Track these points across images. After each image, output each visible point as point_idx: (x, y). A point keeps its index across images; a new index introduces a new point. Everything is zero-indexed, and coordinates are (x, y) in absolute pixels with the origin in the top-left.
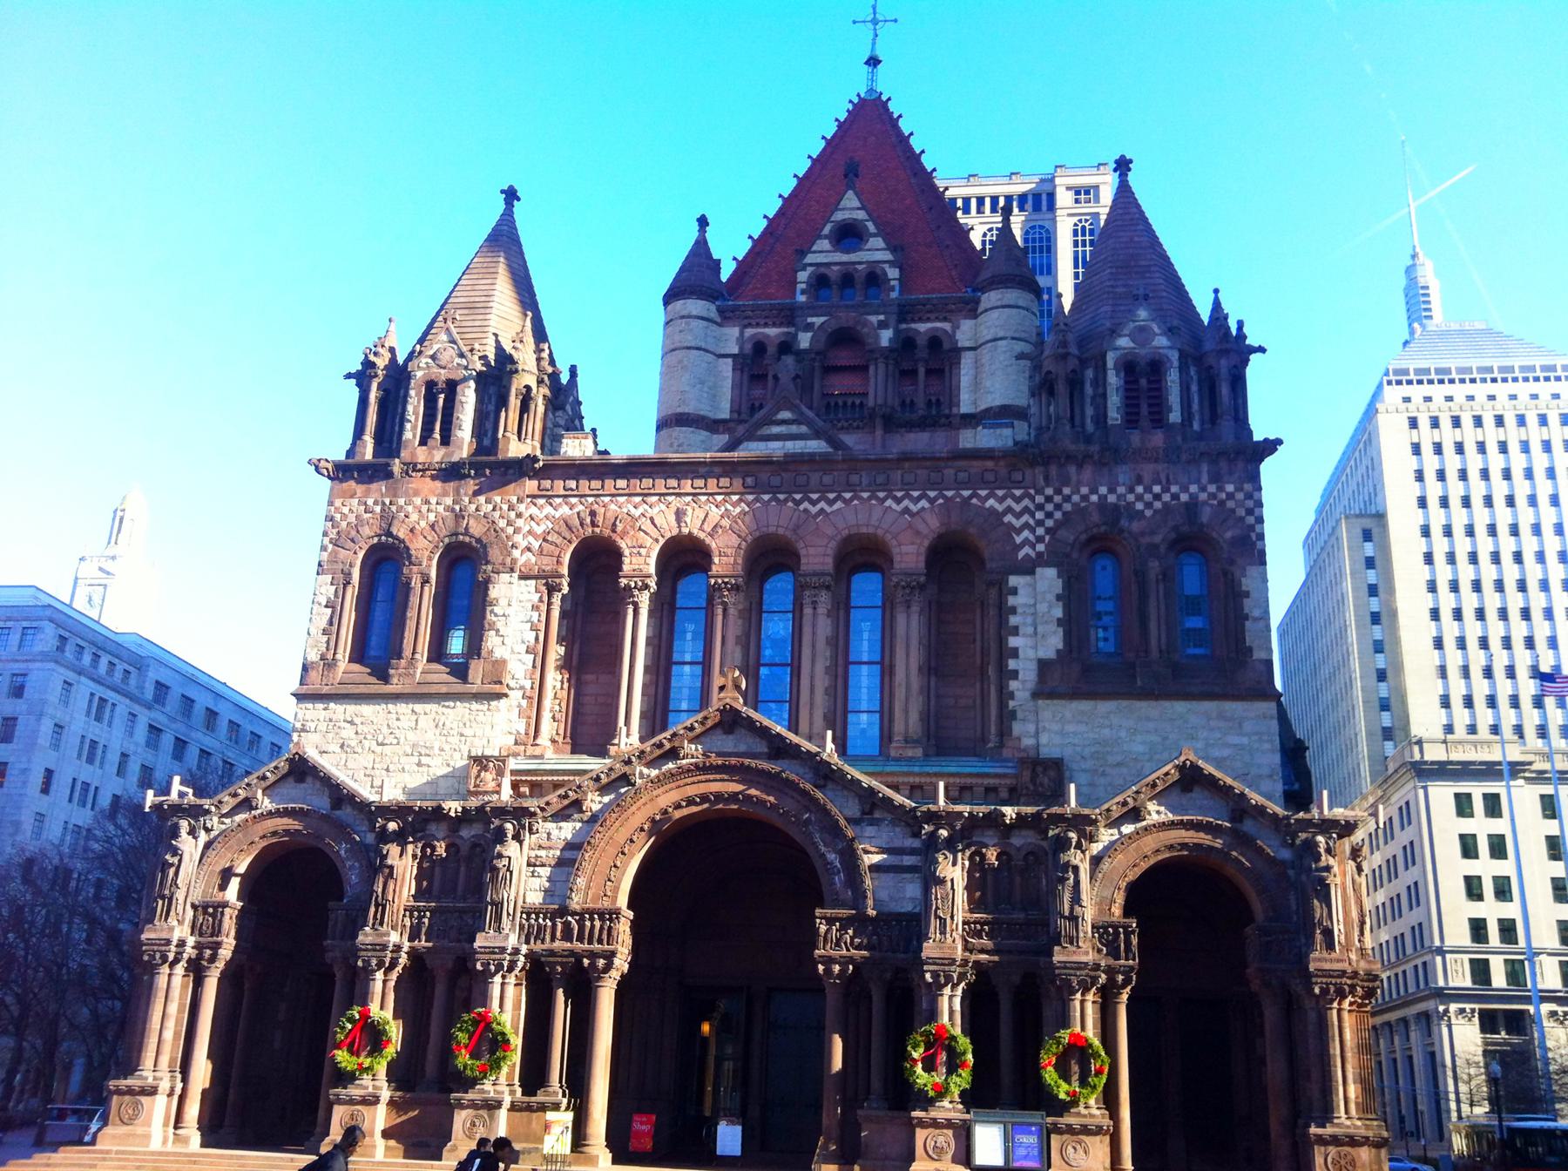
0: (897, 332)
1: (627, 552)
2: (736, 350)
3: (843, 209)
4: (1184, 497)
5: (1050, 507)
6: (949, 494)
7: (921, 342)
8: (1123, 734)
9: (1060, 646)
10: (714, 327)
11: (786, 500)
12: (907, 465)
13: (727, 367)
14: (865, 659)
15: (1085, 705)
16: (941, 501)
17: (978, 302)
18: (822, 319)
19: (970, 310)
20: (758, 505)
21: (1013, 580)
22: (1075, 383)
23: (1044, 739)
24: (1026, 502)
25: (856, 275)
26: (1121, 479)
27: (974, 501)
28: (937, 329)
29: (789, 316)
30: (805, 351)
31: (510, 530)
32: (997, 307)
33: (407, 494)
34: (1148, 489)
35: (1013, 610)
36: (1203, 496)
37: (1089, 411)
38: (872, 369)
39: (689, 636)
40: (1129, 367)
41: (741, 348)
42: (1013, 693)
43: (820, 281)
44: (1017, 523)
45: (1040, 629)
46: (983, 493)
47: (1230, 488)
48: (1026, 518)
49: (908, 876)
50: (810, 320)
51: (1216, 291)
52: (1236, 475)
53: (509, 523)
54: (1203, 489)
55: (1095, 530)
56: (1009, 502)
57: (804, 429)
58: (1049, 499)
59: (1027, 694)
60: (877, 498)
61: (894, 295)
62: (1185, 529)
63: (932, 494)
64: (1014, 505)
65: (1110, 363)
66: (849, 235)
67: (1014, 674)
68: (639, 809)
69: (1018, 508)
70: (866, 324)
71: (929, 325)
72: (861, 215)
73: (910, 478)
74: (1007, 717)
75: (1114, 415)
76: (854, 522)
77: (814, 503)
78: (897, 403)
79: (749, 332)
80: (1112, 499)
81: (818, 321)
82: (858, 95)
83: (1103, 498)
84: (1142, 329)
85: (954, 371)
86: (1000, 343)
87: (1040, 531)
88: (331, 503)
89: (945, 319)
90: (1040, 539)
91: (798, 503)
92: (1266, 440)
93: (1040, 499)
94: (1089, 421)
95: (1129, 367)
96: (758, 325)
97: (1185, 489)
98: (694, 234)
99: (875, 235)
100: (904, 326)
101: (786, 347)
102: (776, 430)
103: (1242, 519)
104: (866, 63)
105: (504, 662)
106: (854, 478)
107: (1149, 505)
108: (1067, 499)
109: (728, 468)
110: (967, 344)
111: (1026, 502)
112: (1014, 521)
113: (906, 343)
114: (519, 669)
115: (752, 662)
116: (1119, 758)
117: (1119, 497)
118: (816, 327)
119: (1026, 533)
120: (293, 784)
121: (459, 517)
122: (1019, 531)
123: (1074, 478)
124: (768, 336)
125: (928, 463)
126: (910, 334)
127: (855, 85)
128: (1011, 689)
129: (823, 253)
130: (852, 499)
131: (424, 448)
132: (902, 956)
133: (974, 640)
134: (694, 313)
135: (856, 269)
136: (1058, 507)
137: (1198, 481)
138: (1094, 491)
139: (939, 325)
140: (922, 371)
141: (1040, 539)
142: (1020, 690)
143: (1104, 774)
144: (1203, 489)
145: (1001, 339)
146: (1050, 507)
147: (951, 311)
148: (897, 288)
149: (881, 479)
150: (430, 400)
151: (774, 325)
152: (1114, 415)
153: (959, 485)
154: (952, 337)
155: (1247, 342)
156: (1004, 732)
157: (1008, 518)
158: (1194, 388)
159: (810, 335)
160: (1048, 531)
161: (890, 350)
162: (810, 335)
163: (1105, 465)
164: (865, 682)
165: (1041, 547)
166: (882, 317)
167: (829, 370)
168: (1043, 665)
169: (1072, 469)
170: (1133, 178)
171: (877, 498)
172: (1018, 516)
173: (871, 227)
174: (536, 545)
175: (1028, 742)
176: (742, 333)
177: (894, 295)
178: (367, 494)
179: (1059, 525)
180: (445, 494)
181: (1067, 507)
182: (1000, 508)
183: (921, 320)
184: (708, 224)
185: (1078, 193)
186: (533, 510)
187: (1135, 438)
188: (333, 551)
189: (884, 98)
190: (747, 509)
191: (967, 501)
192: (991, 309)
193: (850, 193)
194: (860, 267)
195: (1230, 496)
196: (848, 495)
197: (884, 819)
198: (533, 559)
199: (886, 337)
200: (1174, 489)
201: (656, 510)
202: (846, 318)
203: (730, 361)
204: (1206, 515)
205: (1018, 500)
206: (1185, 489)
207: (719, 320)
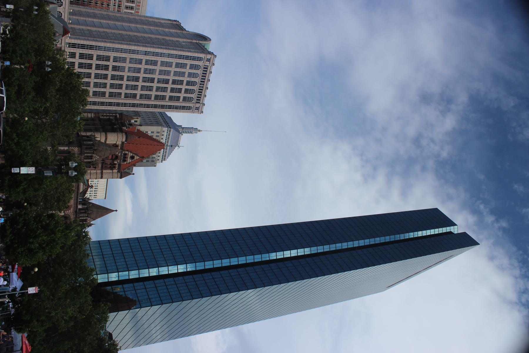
0: (117, 164)
2: (117, 144)
7: (115, 166)
13: (115, 143)
17: (119, 172)
38: (111, 160)
40: (86, 219)
43: (125, 154)
57: (84, 189)
61: (122, 163)
66: (132, 158)
70: (118, 160)
72: (135, 159)
75: (81, 218)
79: (120, 145)
81: (120, 154)
95: (86, 219)
102: (84, 186)
106: (76, 197)
113: (115, 164)
149: (76, 200)
152: (81, 218)
154: (115, 169)
157: (70, 210)
161: (114, 163)
169: (75, 215)
173: (133, 160)
183: (118, 166)
185: (198, 108)
193: (139, 158)
199: (116, 162)
202: (119, 158)
203: (116, 143)
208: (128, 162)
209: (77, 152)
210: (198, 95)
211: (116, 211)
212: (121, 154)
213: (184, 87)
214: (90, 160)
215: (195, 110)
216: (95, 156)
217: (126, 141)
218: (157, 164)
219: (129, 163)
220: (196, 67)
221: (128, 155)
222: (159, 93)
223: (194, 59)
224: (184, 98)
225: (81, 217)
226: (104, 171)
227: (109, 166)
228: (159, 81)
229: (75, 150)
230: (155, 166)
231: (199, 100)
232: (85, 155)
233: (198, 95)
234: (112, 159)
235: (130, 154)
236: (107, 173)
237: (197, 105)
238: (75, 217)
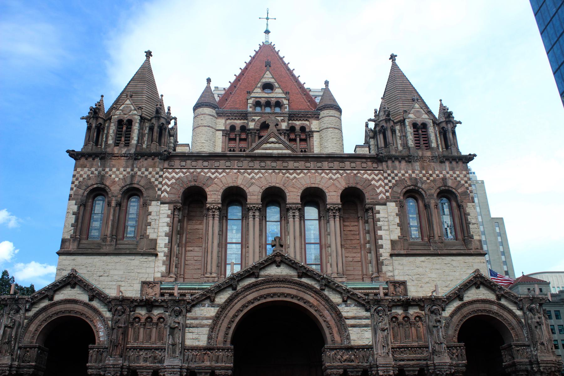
0: (288, 124)
1: (208, 193)
2: (224, 129)
3: (265, 78)
4: (441, 176)
5: (390, 178)
6: (348, 172)
7: (298, 128)
8: (428, 270)
9: (400, 235)
10: (215, 119)
11: (279, 173)
12: (330, 160)
14: (312, 242)
15: (411, 259)
16: (345, 175)
18: (259, 118)
19: (316, 117)
20: (267, 174)
21: (378, 208)
22: (393, 131)
23: (396, 272)
24: (380, 176)
25: (272, 102)
26: (416, 168)
27: (359, 175)
28: (304, 124)
29: (244, 116)
30: (252, 129)
31: (157, 183)
32: (327, 116)
33: (109, 167)
34: (427, 173)
35: (379, 220)
36: (448, 176)
37: (399, 142)
39: (234, 231)
40: (414, 125)
41: (225, 127)
42: (381, 254)
43: (258, 104)
44: (378, 184)
45: (391, 227)
46: (362, 172)
47: (458, 173)
48: (380, 182)
49: (366, 328)
50: (253, 118)
51: (441, 100)
52: (460, 168)
53: (157, 180)
54: (448, 173)
55: (408, 188)
56: (373, 176)
58: (389, 175)
59: (388, 254)
60: (318, 173)
62: (443, 188)
63: (341, 172)
64: (375, 177)
65: (407, 123)
66: (268, 86)
67: (382, 247)
68: (238, 301)
69: (377, 178)
71: (300, 122)
72: (272, 80)
73: (331, 165)
74: (379, 264)
75: (411, 143)
76: (309, 182)
77: (291, 174)
79: (229, 121)
80: (414, 175)
82: (263, 43)
83: (410, 175)
84: (418, 111)
85: (311, 140)
86: (329, 129)
87: (387, 188)
88: (75, 170)
89: (307, 120)
90: (387, 191)
91: (284, 174)
92: (470, 155)
93: (385, 175)
94: (399, 145)
95: (415, 125)
96: (232, 119)
97: (441, 173)
98: (205, 84)
99: (278, 88)
100: (290, 122)
101: (243, 128)
102: (268, 145)
103: (463, 185)
104: (264, 32)
105: (156, 240)
106: (308, 164)
107: (428, 179)
108: (396, 175)
109: (253, 159)
110: (316, 130)
111: (380, 176)
112: (375, 183)
113: (292, 129)
114: (162, 243)
115: (264, 243)
116: (427, 280)
117: (417, 175)
118: (256, 121)
119: (381, 188)
120: (70, 289)
121: (133, 177)
122: (378, 188)
123: (398, 167)
124: (236, 124)
125: (339, 160)
126: (293, 125)
127: (261, 39)
128: (381, 252)
129: (258, 93)
130: (307, 173)
131: (118, 147)
132: (366, 364)
133: (359, 234)
134: (207, 113)
135: (271, 100)
136: (393, 178)
137: (445, 170)
138: (407, 172)
139: (303, 122)
140: (298, 139)
141: (387, 191)
142: (385, 252)
143: (421, 287)
144: (448, 173)
145: (329, 128)
146: (390, 178)
147: (309, 117)
148: (288, 107)
151: (239, 119)
153: (353, 169)
155: (455, 119)
156: (379, 271)
157: (373, 182)
158: (438, 135)
159: (254, 123)
160: (390, 188)
161: (287, 130)
162: (254, 123)
163: (410, 162)
164: (313, 251)
165: (388, 194)
166: (282, 118)
168: (393, 243)
169: (397, 163)
170: (397, 62)
171: (318, 173)
172: (377, 181)
174: (168, 189)
175: (390, 274)
176: (226, 122)
177: (287, 110)
178: (92, 166)
179: (395, 185)
180: (127, 167)
181: (397, 178)
182: (370, 178)
183: (297, 120)
184: (211, 81)
186: (167, 174)
187: (420, 153)
188: (76, 190)
189: (272, 44)
190: (262, 176)
191: (355, 175)
192: (325, 117)
193: (268, 72)
194: (273, 99)
195: (458, 176)
196: (306, 171)
197: (352, 304)
198: (167, 195)
199: (284, 126)
200: (437, 172)
201: (222, 175)
203: (221, 132)
204: (450, 183)
205: (377, 175)
206: (441, 173)
207: (216, 116)
208: (284, 96)
209: (93, 169)
211: (393, 57)
212: (256, 114)
214: (136, 127)
216: (118, 112)
218: (478, 179)
221: (260, 98)
225: (405, 145)
229: (85, 176)
230: (483, 182)
232: (110, 142)
238: (403, 163)
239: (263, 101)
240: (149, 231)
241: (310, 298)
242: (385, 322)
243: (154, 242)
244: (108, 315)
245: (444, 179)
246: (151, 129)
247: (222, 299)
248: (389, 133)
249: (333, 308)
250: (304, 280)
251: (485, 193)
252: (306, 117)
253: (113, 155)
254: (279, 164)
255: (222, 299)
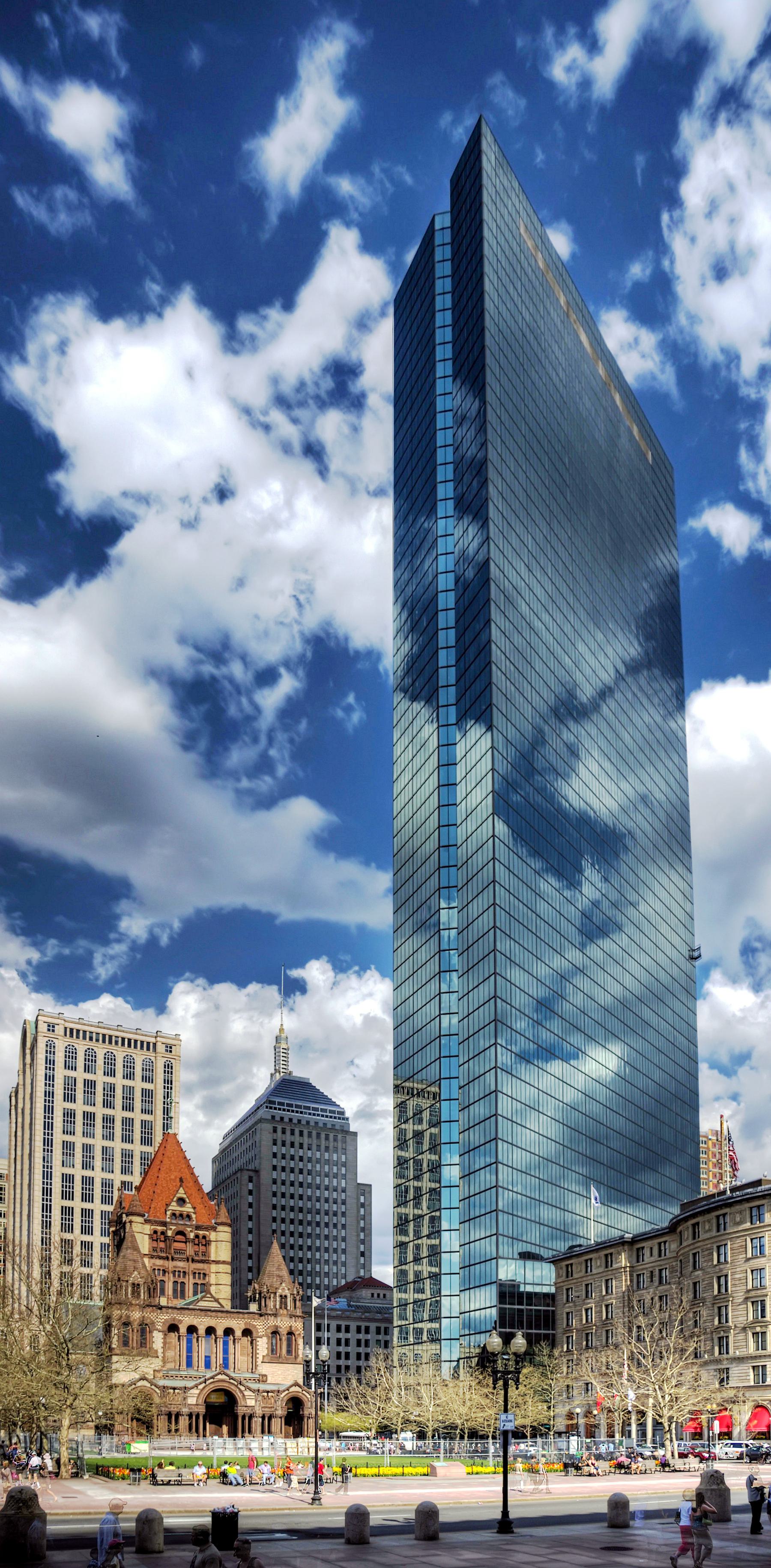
13: (147, 1237)
29: (164, 1224)
40: (281, 1296)
43: (174, 1214)
72: (184, 1196)
74: (256, 1366)
75: (278, 1307)
78: (193, 1254)
79: (153, 1227)
81: (173, 1228)
95: (281, 1296)
101: (163, 1233)
113: (197, 1236)
114: (160, 1351)
129: (174, 1207)
150: (133, 1288)
167: (175, 1241)
173: (187, 1200)
187: (281, 1311)
199: (192, 1236)
202: (181, 1228)
210: (135, 1047)
213: (119, 1081)
215: (173, 1053)
217: (143, 1216)
219: (194, 1208)
220: (71, 1055)
222: (137, 1135)
223: (50, 1063)
224: (145, 1079)
225: (275, 1306)
226: (213, 1258)
227: (202, 1248)
228: (110, 1137)
231: (148, 1044)
232: (130, 1296)
233: (135, 1047)
234: (186, 1243)
235: (174, 1207)
236: (216, 1252)
237: (161, 1048)
239: (177, 1213)
240: (154, 1346)
241: (233, 1387)
242: (260, 1398)
243: (156, 1351)
244: (158, 1391)
245: (291, 1327)
246: (149, 1289)
247: (201, 1387)
248: (268, 1300)
249: (241, 1391)
250: (232, 1381)
251: (356, 1149)
252: (207, 1229)
253: (131, 1304)
254: (214, 1314)
255: (201, 1387)
